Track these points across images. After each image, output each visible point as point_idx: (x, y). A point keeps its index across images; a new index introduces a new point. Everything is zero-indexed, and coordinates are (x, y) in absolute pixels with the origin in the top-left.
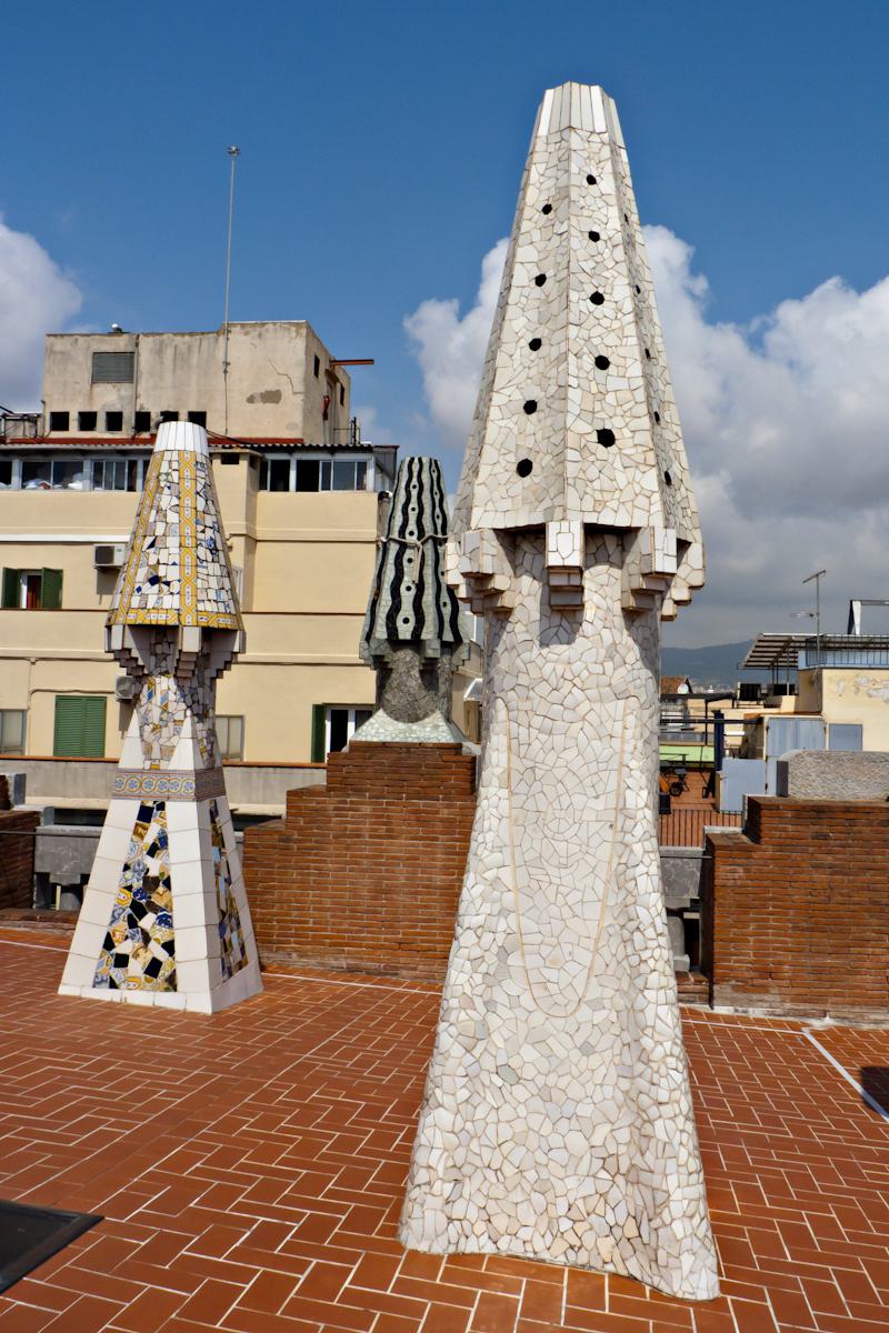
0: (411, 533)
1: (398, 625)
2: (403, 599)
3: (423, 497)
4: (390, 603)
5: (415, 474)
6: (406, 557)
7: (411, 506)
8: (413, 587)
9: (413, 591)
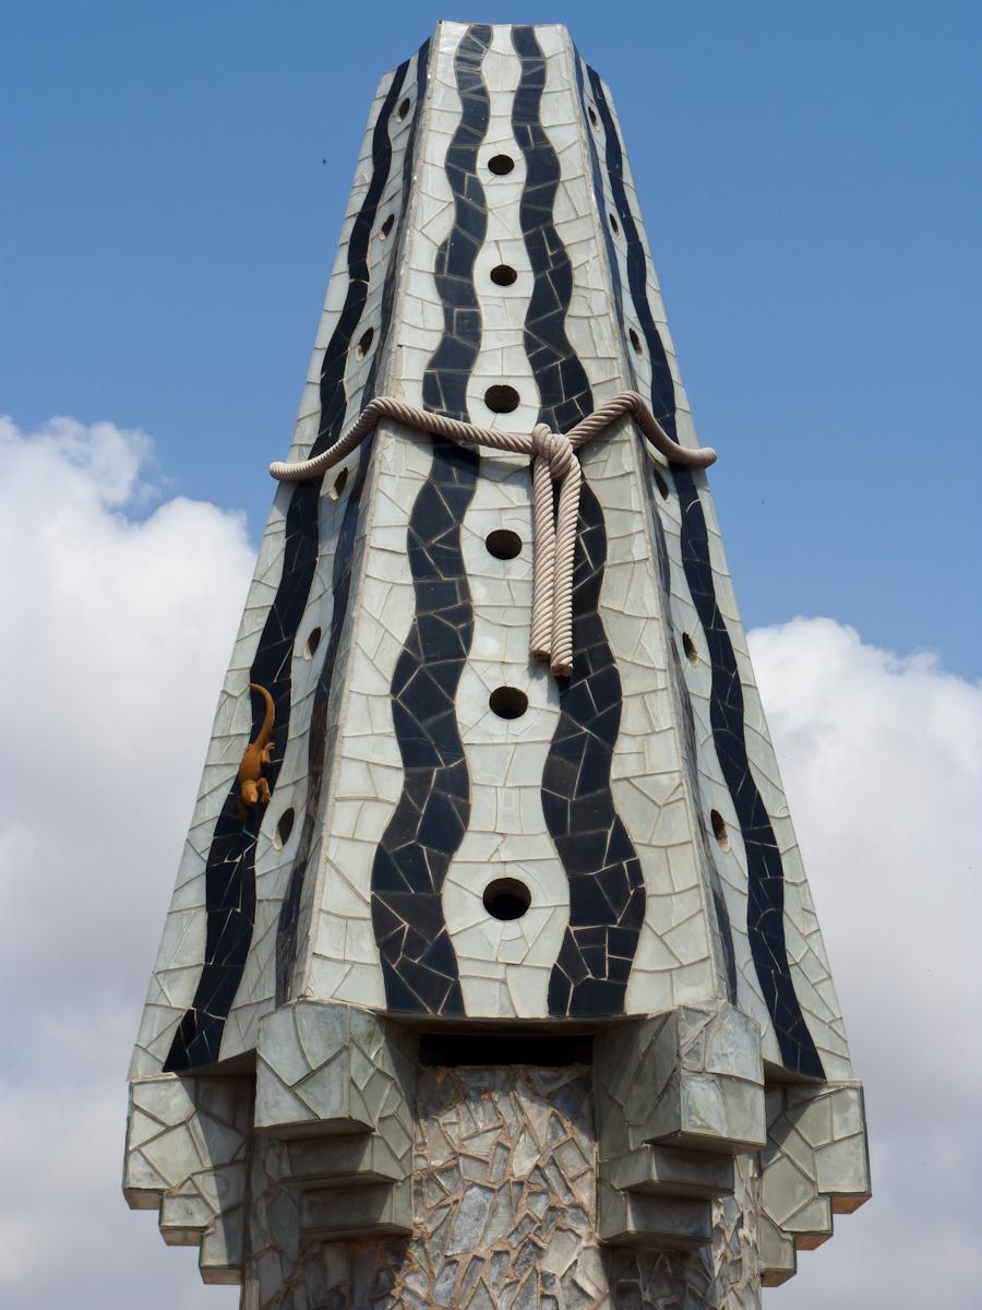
0: (502, 400)
1: (452, 925)
2: (478, 765)
3: (560, 213)
4: (393, 786)
5: (501, 108)
6: (477, 523)
7: (484, 263)
8: (538, 692)
9: (543, 716)
